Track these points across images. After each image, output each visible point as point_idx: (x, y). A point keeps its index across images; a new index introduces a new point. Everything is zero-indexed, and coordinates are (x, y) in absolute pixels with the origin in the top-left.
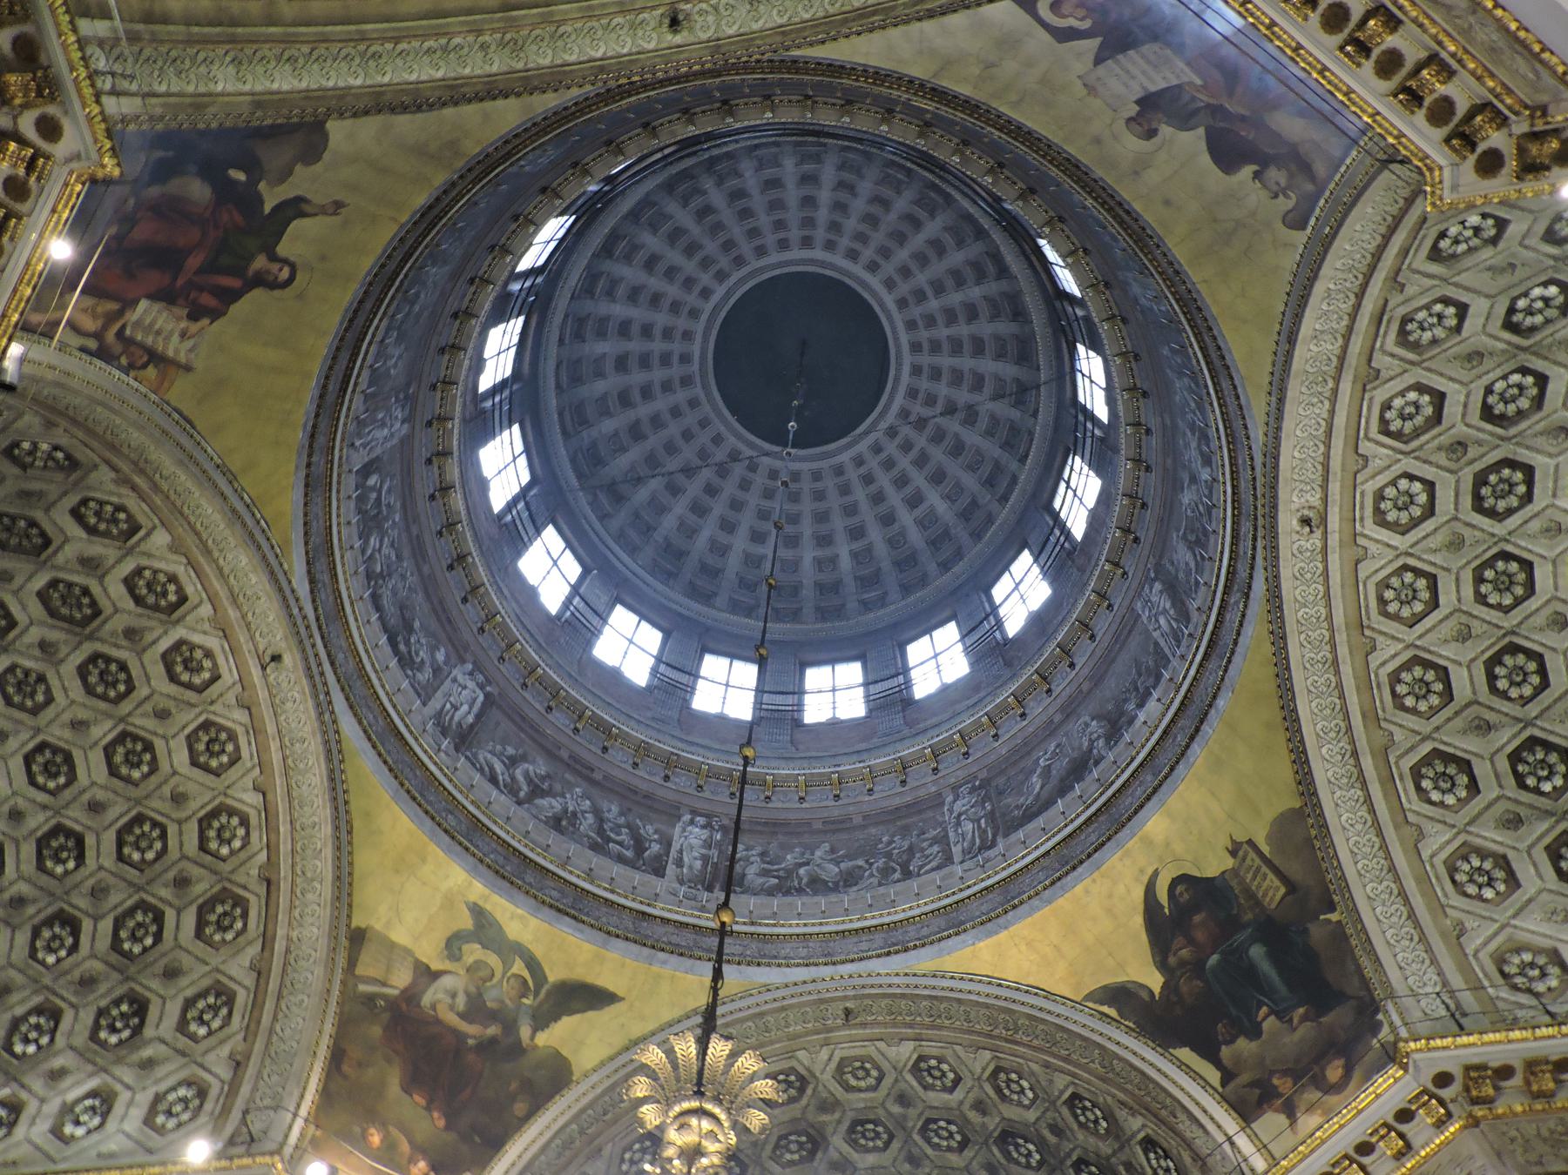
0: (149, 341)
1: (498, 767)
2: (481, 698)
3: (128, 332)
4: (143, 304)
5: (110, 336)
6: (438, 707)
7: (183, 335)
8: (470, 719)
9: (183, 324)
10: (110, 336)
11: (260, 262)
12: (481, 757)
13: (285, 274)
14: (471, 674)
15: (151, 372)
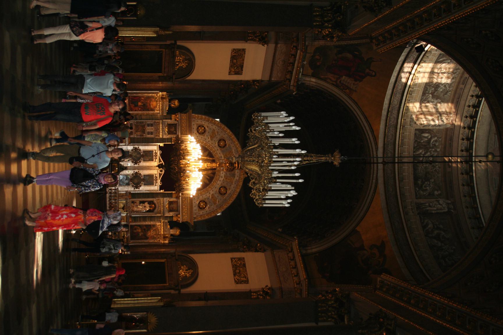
0: (347, 84)
1: (430, 226)
2: (446, 210)
3: (342, 82)
4: (344, 77)
5: (338, 82)
6: (422, 202)
7: (354, 84)
8: (434, 212)
9: (353, 82)
10: (338, 82)
11: (367, 71)
12: (426, 221)
13: (374, 74)
14: (448, 204)
15: (348, 91)
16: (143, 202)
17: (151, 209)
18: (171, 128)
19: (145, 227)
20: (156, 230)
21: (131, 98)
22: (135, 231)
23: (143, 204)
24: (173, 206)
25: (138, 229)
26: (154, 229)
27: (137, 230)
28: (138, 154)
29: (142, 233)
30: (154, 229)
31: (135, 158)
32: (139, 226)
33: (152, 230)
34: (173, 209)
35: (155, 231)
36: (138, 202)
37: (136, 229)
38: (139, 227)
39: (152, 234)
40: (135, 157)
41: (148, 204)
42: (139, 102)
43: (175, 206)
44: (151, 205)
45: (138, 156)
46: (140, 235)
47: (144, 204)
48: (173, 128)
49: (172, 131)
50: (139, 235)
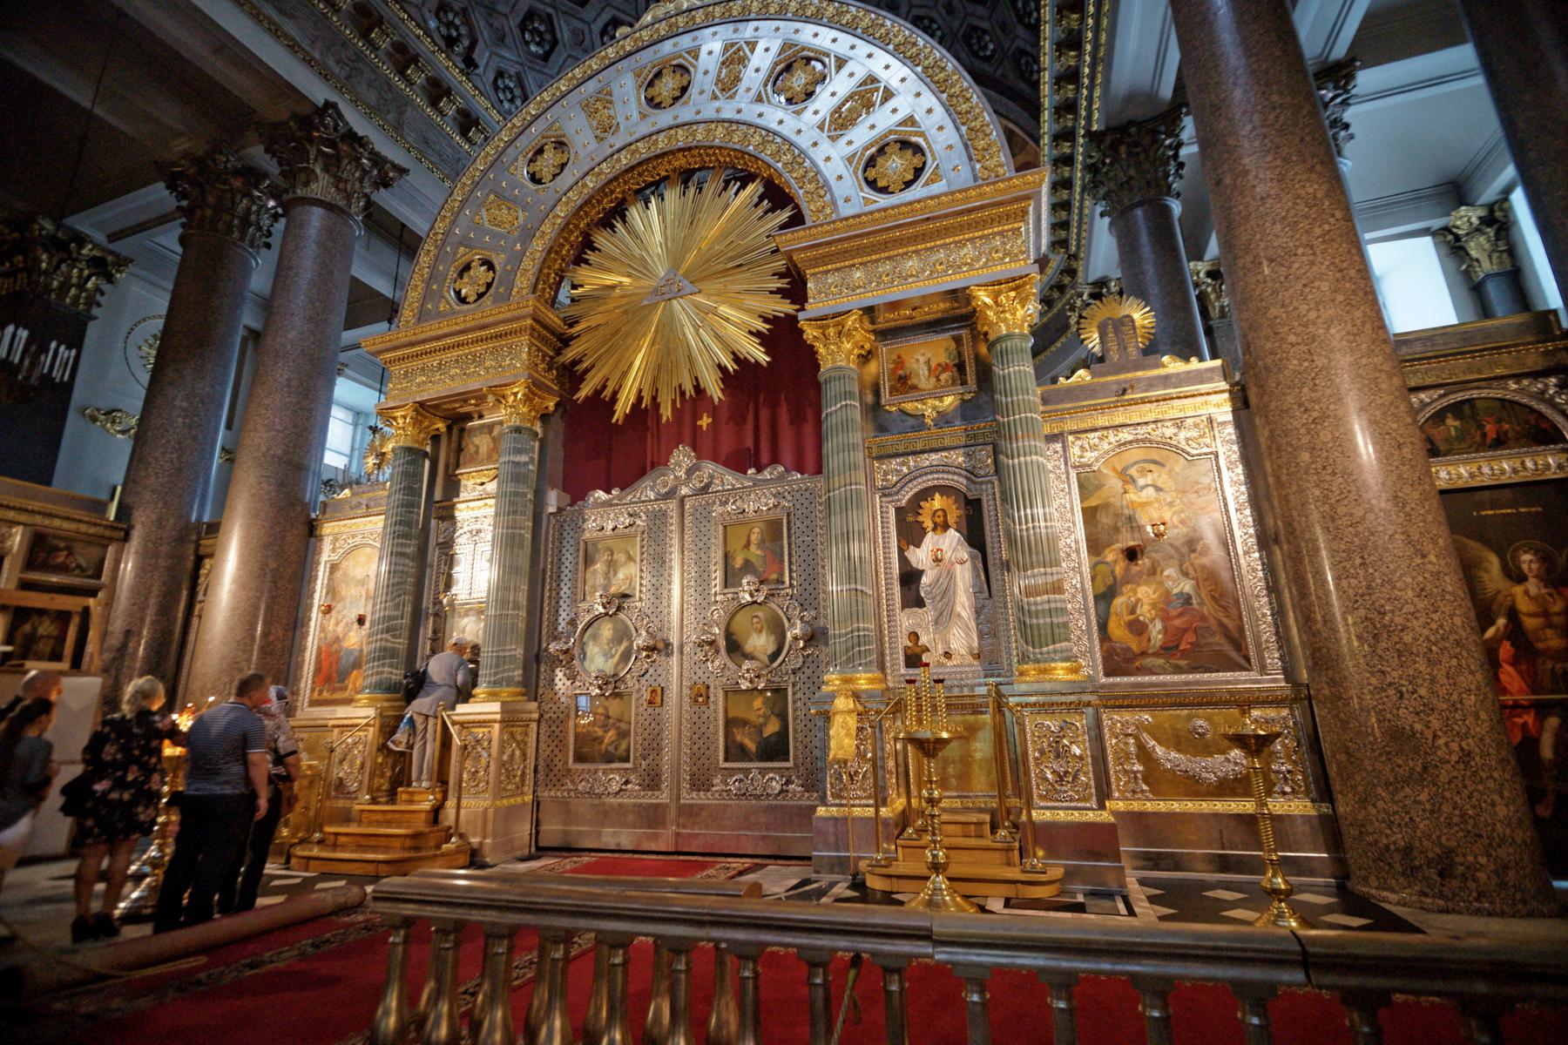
16: (910, 577)
17: (954, 515)
18: (477, 452)
19: (1110, 556)
20: (1126, 469)
21: (321, 692)
22: (1156, 631)
23: (924, 580)
24: (923, 371)
25: (1133, 612)
26: (1114, 483)
27: (1144, 612)
28: (595, 637)
29: (1170, 572)
30: (1114, 483)
31: (617, 656)
32: (1105, 597)
33: (1132, 496)
34: (945, 368)
35: (1133, 471)
36: (906, 620)
37: (1138, 628)
38: (1119, 602)
39: (1158, 489)
40: (608, 655)
41: (918, 546)
42: (345, 644)
43: (922, 359)
44: (928, 524)
45: (606, 630)
46: (1187, 586)
47: (918, 574)
48: (477, 440)
49: (491, 445)
50: (1187, 600)
